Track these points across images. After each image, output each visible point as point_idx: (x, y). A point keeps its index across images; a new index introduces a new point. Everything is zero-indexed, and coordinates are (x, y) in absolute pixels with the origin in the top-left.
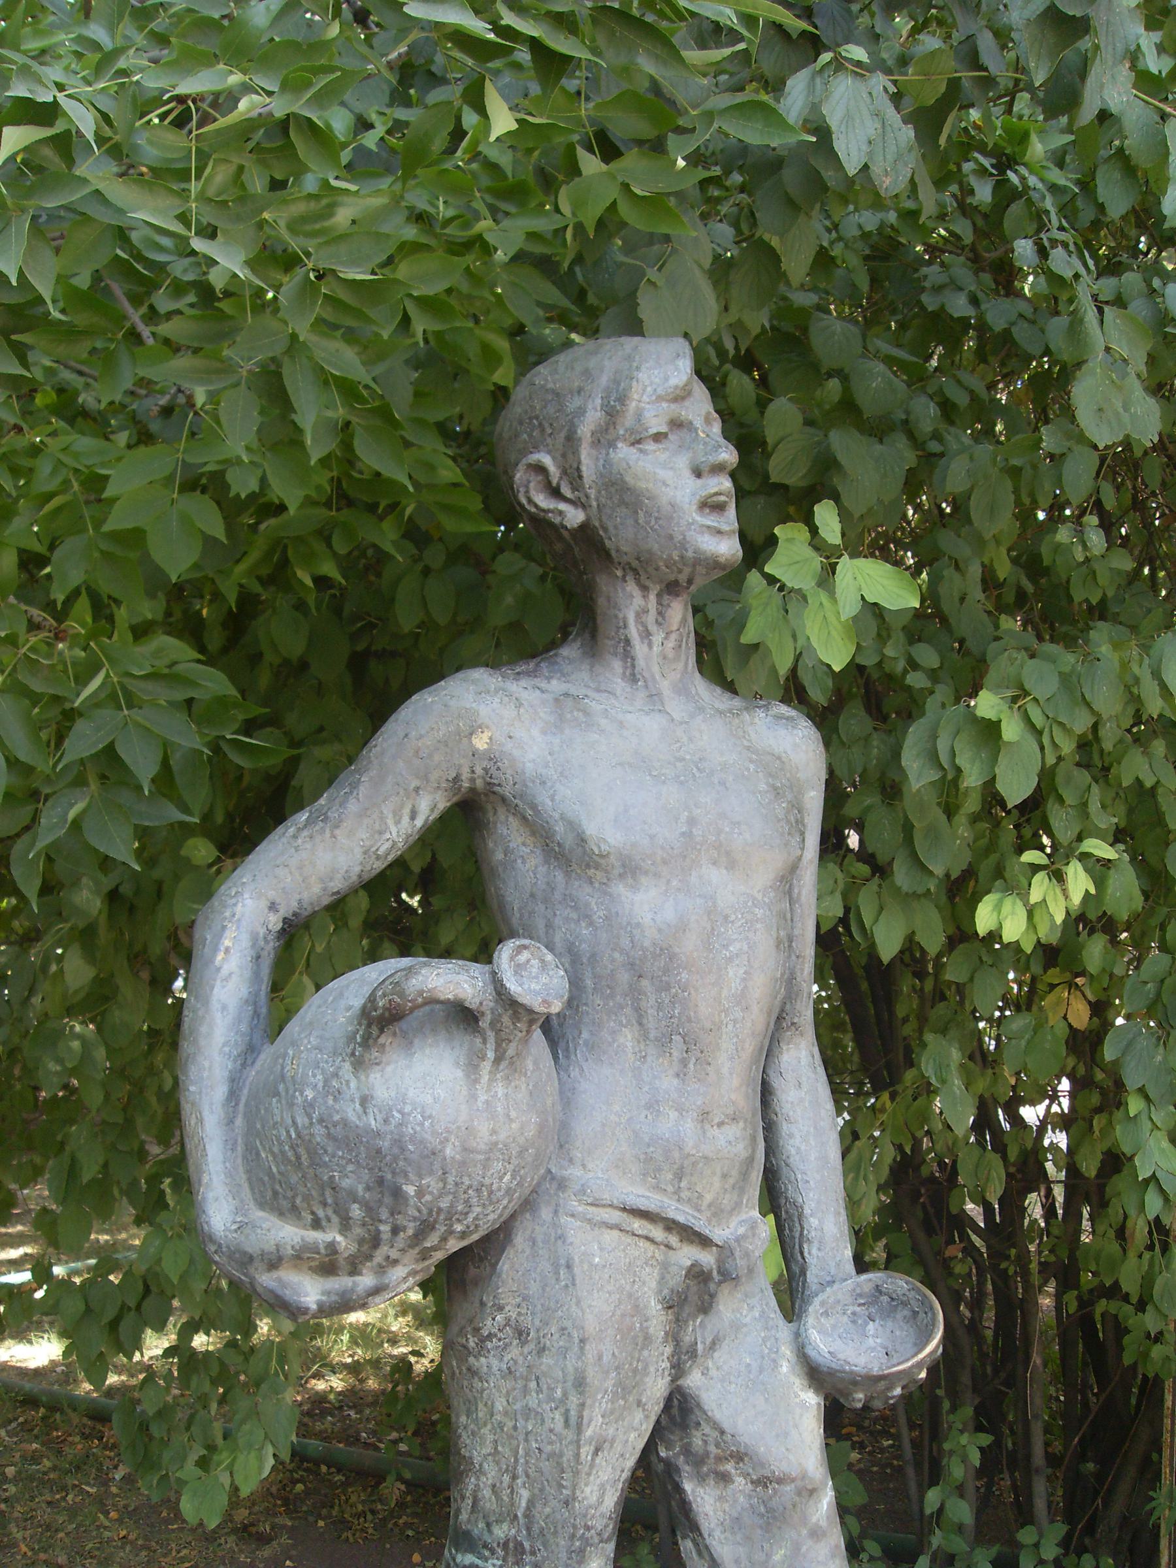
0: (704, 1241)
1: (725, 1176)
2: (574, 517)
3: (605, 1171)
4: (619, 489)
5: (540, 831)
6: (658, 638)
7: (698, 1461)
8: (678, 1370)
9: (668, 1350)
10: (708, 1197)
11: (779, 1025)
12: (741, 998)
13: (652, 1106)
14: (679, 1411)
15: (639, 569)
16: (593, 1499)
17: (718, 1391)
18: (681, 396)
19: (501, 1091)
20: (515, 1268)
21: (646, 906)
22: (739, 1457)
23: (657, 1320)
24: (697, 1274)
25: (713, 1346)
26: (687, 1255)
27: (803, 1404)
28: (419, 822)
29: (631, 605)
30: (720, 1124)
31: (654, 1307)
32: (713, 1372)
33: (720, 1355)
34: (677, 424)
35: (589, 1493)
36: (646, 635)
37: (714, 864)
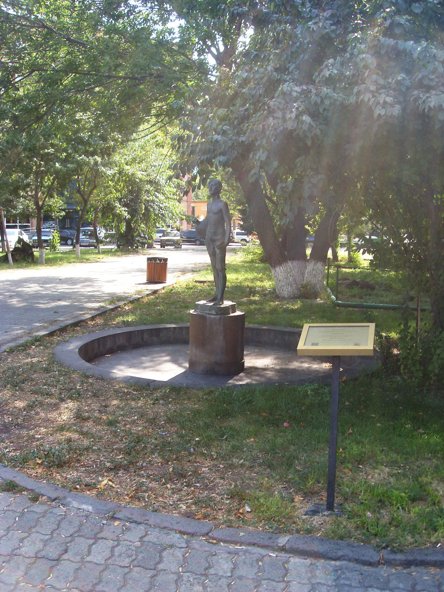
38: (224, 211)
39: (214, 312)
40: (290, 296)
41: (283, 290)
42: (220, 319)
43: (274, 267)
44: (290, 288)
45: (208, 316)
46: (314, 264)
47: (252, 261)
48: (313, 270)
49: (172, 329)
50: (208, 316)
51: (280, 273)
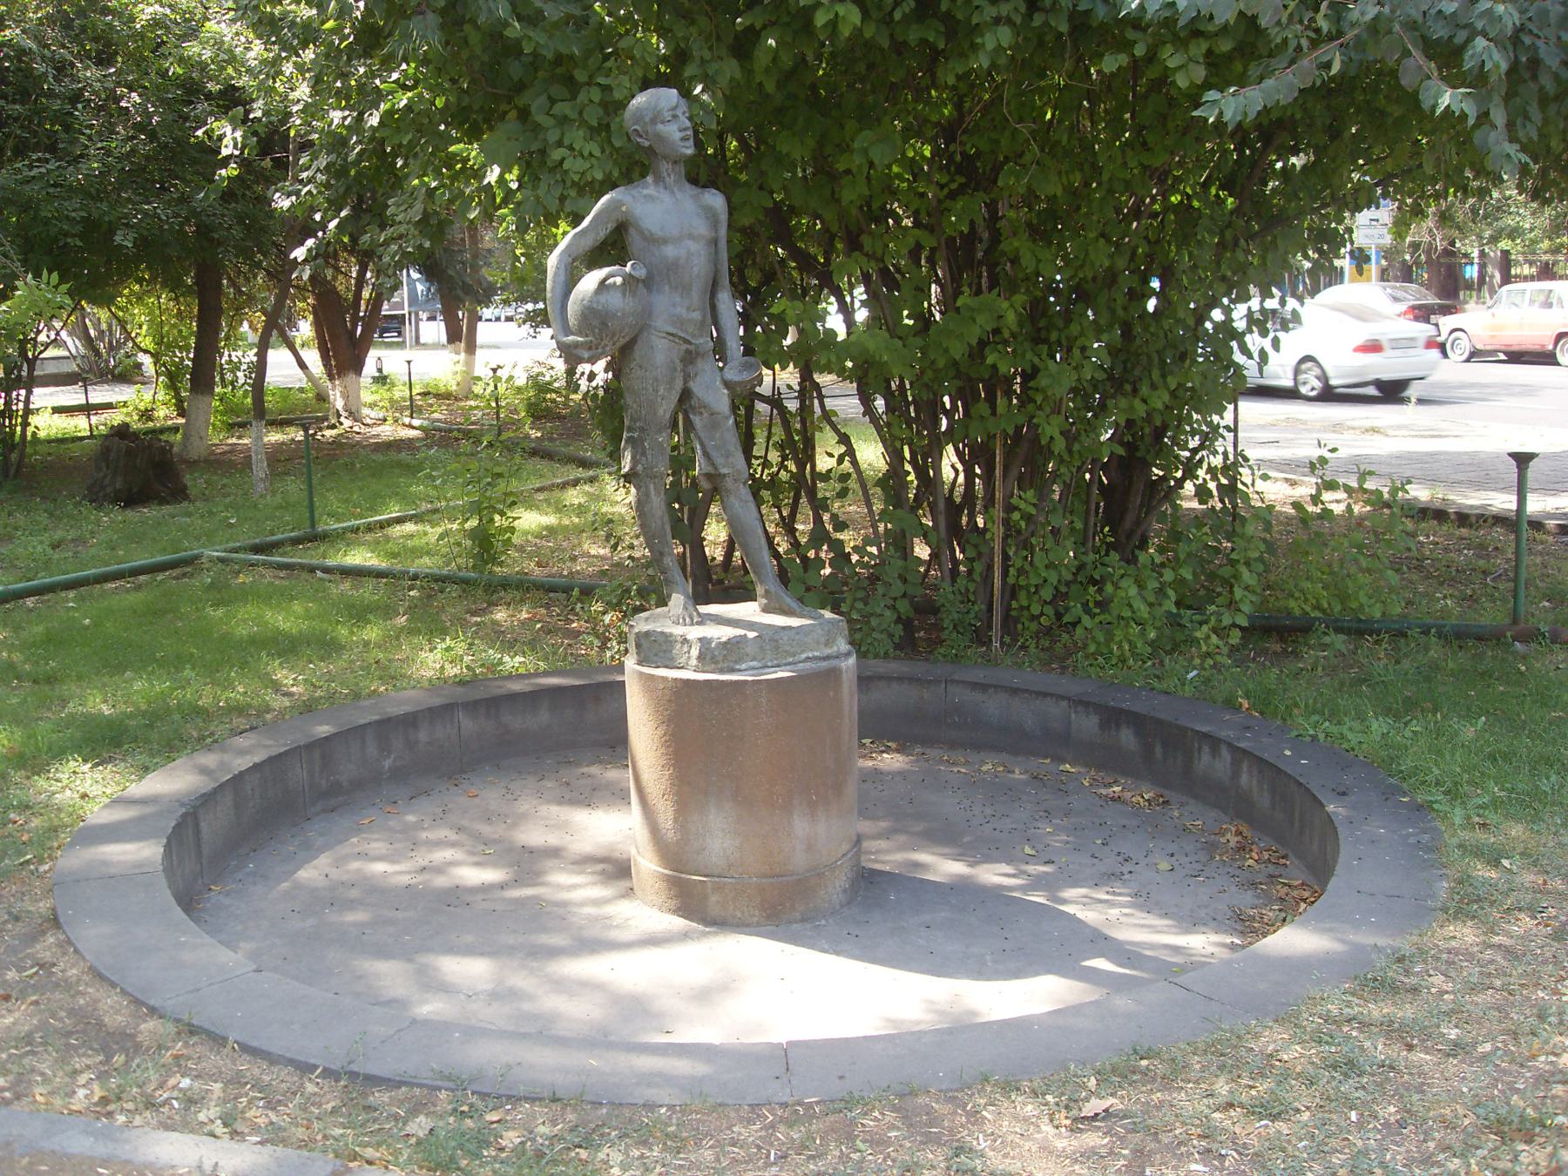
0: (689, 343)
2: (647, 144)
3: (661, 323)
4: (660, 138)
5: (641, 232)
7: (693, 408)
8: (686, 382)
11: (714, 288)
13: (674, 305)
14: (686, 395)
15: (665, 158)
17: (696, 388)
18: (675, 108)
20: (638, 351)
21: (670, 251)
23: (679, 366)
24: (688, 352)
26: (685, 347)
29: (665, 167)
34: (675, 116)
35: (661, 412)
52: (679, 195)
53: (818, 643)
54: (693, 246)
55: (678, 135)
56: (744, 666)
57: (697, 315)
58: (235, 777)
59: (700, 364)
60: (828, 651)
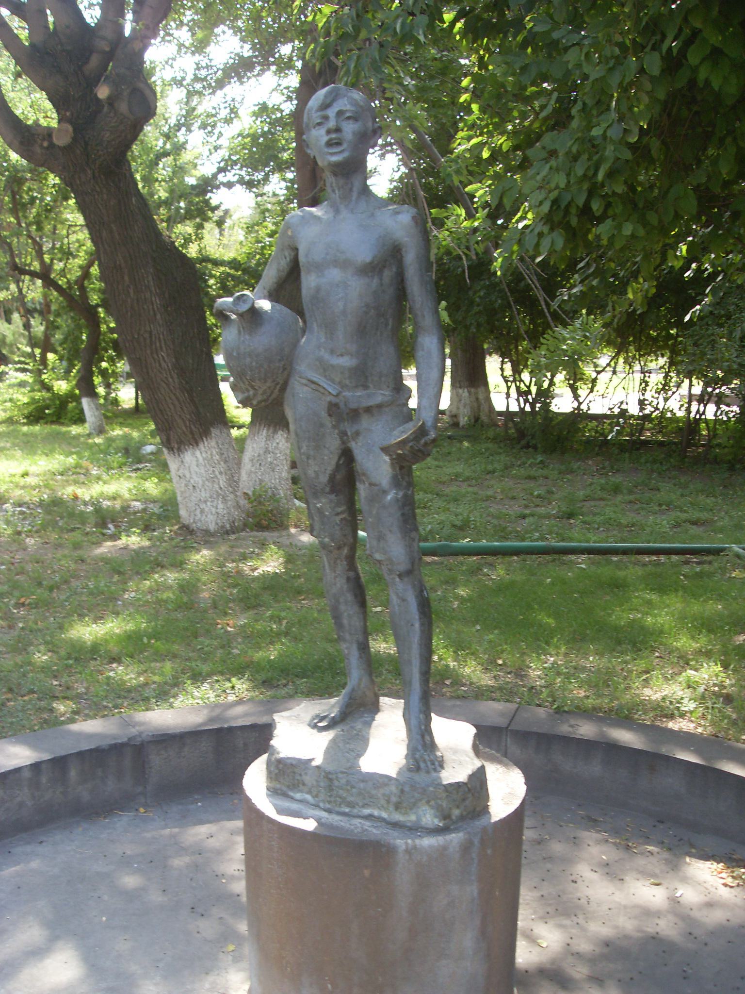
1: (342, 373)
6: (337, 191)
9: (336, 431)
10: (337, 380)
12: (344, 312)
16: (313, 475)
19: (247, 337)
22: (364, 474)
25: (357, 434)
27: (385, 462)
28: (288, 259)
30: (342, 355)
31: (324, 414)
32: (360, 444)
33: (361, 438)
34: (326, 118)
36: (333, 191)
37: (335, 267)
38: (410, 258)
39: (429, 818)
40: (223, 527)
41: (202, 511)
42: (466, 848)
43: (179, 449)
44: (221, 506)
45: (401, 842)
46: (268, 438)
47: (10, 421)
48: (267, 451)
49: (27, 774)
50: (401, 842)
51: (194, 468)
52: (344, 213)
53: (388, 802)
54: (335, 274)
55: (325, 138)
56: (298, 796)
57: (346, 362)
58: (219, 730)
59: (365, 422)
60: (398, 817)
